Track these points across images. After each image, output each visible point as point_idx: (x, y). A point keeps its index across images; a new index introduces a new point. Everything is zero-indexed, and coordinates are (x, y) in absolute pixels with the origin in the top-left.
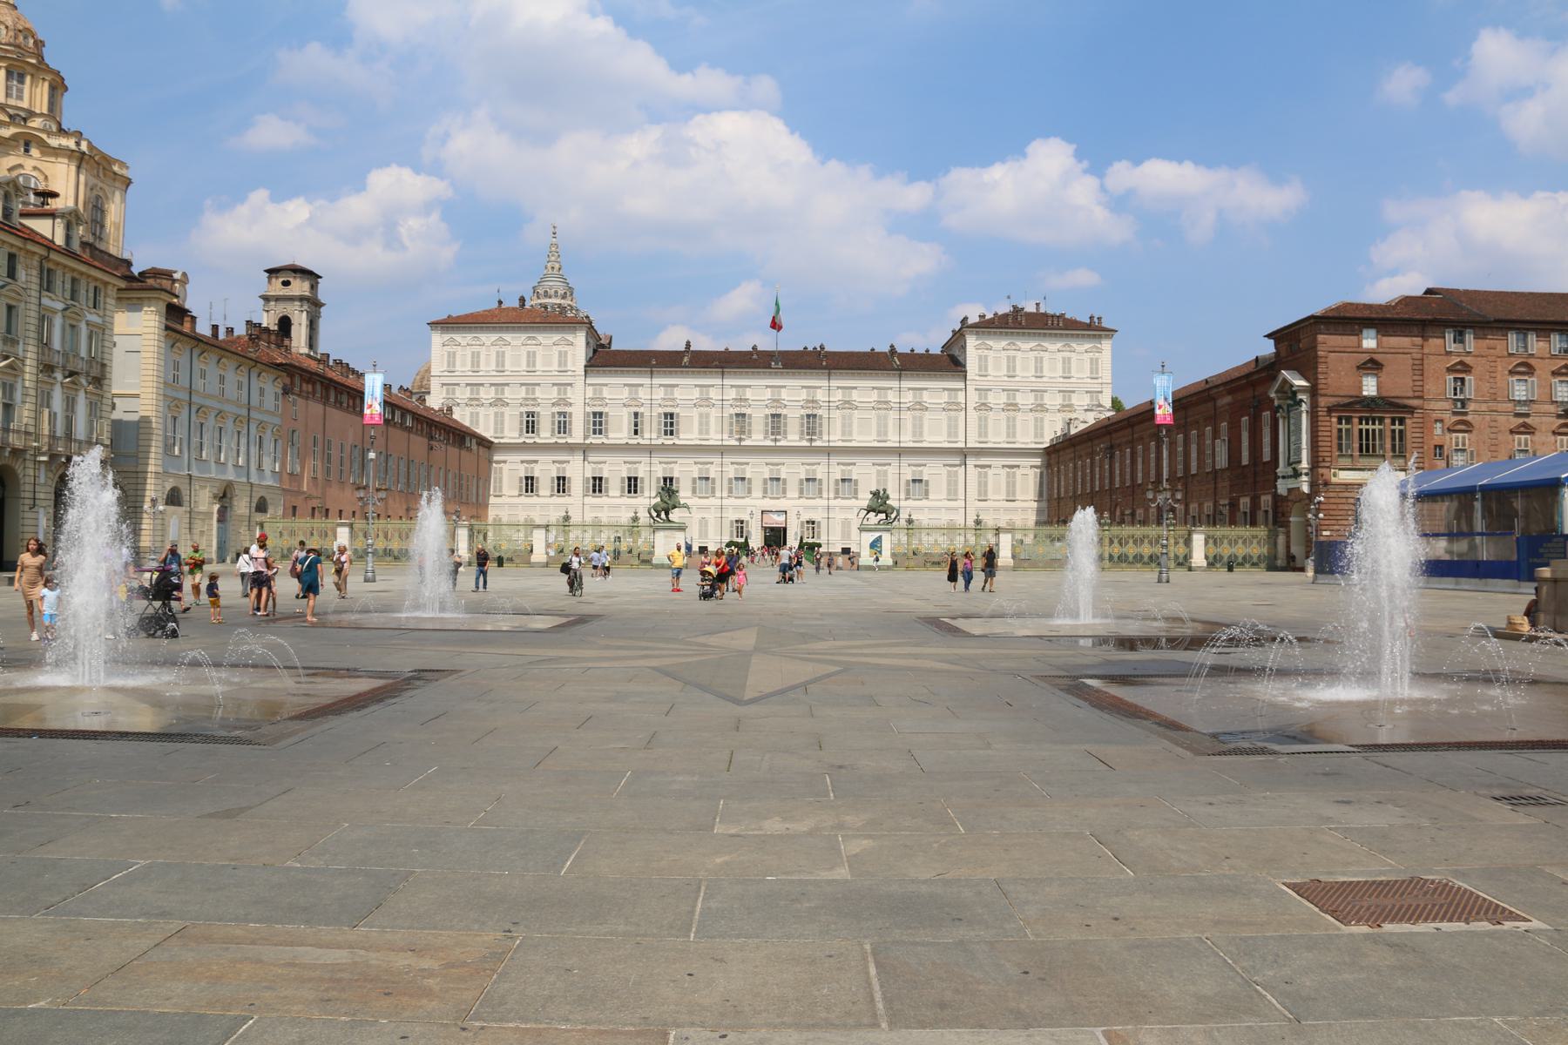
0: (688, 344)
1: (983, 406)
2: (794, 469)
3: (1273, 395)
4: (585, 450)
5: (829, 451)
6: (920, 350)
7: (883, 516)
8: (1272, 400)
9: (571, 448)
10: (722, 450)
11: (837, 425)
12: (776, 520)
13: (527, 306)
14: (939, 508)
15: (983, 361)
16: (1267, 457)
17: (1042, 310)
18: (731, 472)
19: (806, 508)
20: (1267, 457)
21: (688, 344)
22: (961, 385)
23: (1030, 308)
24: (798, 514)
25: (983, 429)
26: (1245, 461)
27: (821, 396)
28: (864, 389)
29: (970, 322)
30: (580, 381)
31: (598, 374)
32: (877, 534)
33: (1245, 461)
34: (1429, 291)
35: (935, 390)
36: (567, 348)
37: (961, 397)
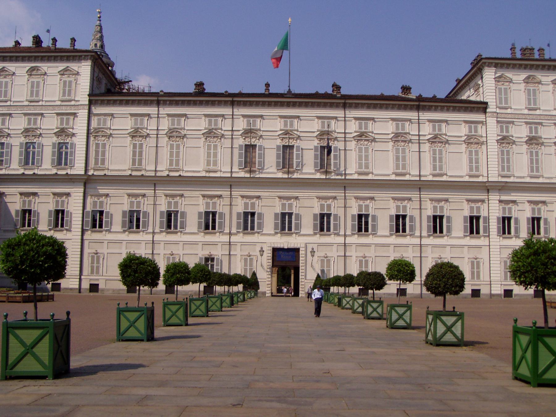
1: (505, 140)
2: (307, 206)
4: (87, 181)
5: (346, 185)
9: (71, 180)
10: (231, 183)
11: (353, 156)
13: (44, 45)
14: (462, 246)
18: (240, 207)
19: (320, 245)
22: (479, 117)
24: (313, 252)
25: (505, 162)
27: (337, 127)
28: (384, 123)
31: (103, 103)
35: (456, 125)
36: (72, 78)
37: (481, 131)
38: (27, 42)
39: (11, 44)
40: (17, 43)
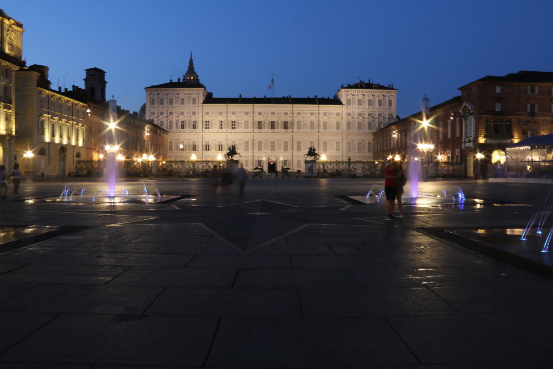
0: (240, 95)
3: (461, 111)
6: (326, 97)
7: (313, 157)
8: (460, 113)
12: (273, 159)
15: (349, 102)
16: (458, 135)
17: (371, 83)
20: (458, 135)
21: (240, 95)
22: (341, 109)
23: (367, 82)
26: (449, 136)
29: (345, 86)
30: (201, 109)
32: (311, 164)
33: (449, 136)
34: (520, 72)
38: (175, 80)
39: (169, 81)
40: (171, 80)
